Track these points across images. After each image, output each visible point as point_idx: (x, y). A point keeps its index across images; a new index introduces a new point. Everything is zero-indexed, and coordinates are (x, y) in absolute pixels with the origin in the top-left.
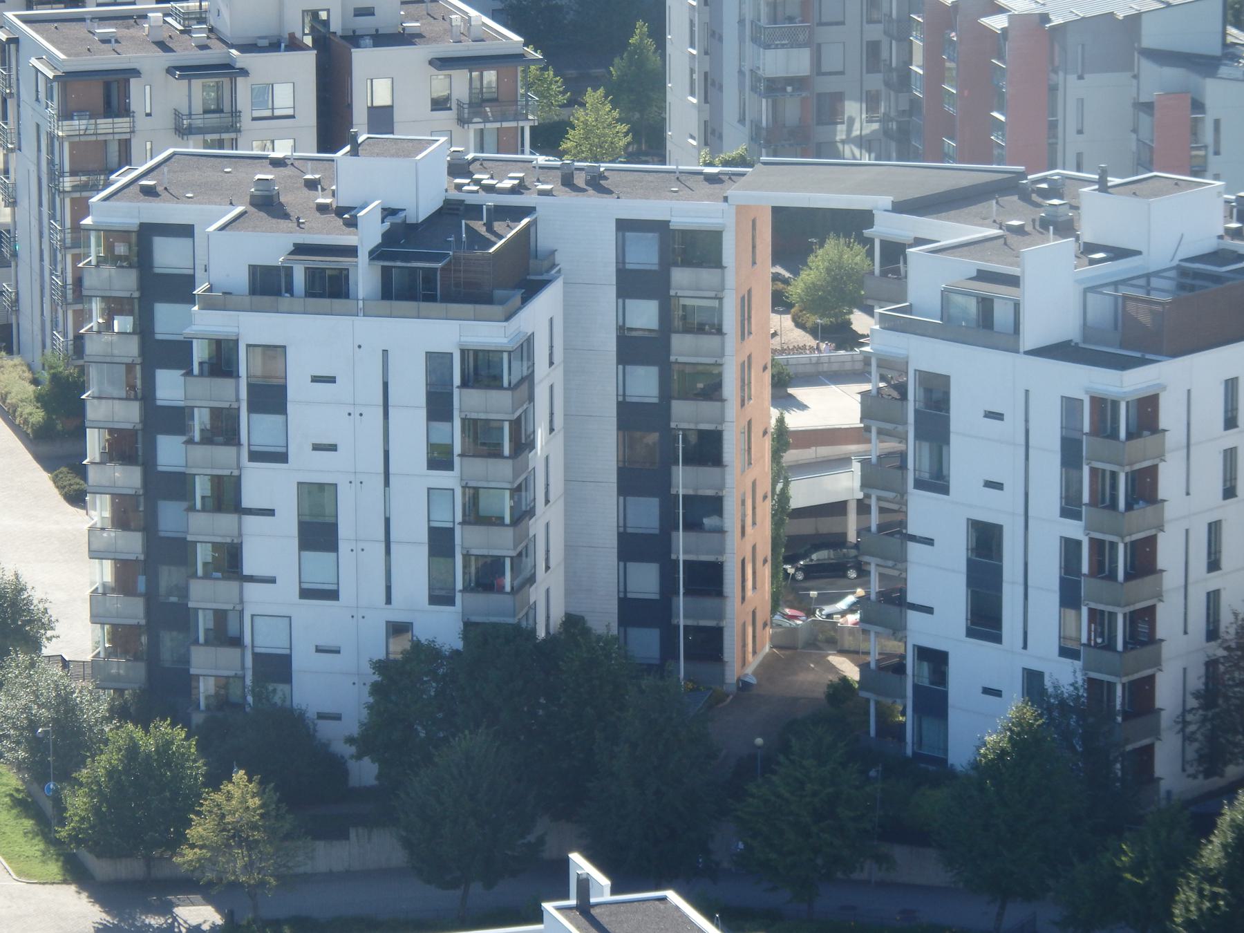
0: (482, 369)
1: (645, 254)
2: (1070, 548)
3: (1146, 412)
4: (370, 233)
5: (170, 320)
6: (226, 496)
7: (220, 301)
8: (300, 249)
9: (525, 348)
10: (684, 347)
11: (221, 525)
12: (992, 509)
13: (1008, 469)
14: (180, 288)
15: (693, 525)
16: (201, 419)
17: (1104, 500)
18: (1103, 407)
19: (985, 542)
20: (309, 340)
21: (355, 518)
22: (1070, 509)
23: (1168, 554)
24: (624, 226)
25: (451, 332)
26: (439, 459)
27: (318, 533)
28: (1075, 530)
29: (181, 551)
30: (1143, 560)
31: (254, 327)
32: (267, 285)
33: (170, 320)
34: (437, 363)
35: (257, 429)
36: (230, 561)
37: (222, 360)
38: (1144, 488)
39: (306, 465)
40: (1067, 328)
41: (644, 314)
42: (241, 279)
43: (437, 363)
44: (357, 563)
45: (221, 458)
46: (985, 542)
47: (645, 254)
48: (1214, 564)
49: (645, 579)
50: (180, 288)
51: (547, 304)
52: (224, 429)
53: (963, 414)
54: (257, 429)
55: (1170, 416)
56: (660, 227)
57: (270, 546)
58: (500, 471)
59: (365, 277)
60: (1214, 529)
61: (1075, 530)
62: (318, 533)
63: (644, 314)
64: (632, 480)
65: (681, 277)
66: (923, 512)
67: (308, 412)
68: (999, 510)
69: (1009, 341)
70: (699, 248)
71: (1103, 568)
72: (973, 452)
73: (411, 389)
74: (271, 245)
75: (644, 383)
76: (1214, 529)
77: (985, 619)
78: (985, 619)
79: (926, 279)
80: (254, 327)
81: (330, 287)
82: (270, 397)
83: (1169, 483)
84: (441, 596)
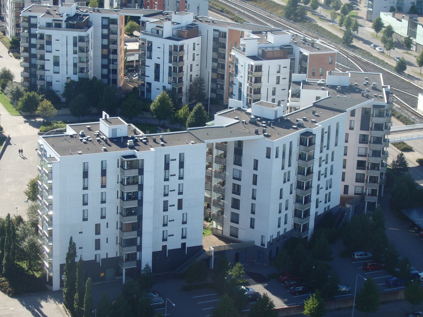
0: (82, 39)
1: (106, 22)
2: (170, 67)
3: (182, 47)
4: (65, 18)
5: (33, 30)
6: (42, 58)
8: (54, 20)
9: (88, 36)
11: (42, 62)
13: (161, 56)
14: (35, 26)
15: (113, 63)
16: (38, 46)
17: (175, 61)
18: (175, 47)
19: (157, 66)
20: (55, 34)
21: (62, 61)
22: (170, 62)
23: (185, 69)
24: (103, 18)
25: (77, 33)
26: (75, 52)
27: (56, 63)
28: (171, 65)
29: (35, 66)
30: (181, 70)
31: (47, 32)
32: (49, 25)
33: (33, 30)
34: (75, 38)
35: (47, 47)
36: (43, 68)
37: (42, 37)
38: (181, 59)
39: (55, 53)
40: (170, 35)
41: (106, 31)
42: (45, 25)
43: (75, 38)
44: (62, 68)
45: (42, 52)
46: (157, 66)
47: (106, 22)
48: (191, 71)
49: (105, 71)
50: (35, 26)
51: (91, 30)
52: (42, 47)
53: (154, 48)
54: (47, 47)
55: (185, 48)
56: (108, 18)
57: (49, 65)
58: (84, 55)
59: (64, 25)
60: (191, 65)
61: (171, 65)
62: (56, 63)
64: (104, 57)
65: (111, 26)
66: (148, 62)
67: (55, 45)
69: (161, 36)
70: (114, 22)
71: (175, 70)
72: (156, 53)
73: (71, 42)
74: (49, 20)
76: (191, 65)
77: (157, 78)
78: (157, 78)
79: (149, 27)
80: (47, 32)
81: (58, 26)
82: (49, 43)
83: (185, 58)
84: (75, 73)
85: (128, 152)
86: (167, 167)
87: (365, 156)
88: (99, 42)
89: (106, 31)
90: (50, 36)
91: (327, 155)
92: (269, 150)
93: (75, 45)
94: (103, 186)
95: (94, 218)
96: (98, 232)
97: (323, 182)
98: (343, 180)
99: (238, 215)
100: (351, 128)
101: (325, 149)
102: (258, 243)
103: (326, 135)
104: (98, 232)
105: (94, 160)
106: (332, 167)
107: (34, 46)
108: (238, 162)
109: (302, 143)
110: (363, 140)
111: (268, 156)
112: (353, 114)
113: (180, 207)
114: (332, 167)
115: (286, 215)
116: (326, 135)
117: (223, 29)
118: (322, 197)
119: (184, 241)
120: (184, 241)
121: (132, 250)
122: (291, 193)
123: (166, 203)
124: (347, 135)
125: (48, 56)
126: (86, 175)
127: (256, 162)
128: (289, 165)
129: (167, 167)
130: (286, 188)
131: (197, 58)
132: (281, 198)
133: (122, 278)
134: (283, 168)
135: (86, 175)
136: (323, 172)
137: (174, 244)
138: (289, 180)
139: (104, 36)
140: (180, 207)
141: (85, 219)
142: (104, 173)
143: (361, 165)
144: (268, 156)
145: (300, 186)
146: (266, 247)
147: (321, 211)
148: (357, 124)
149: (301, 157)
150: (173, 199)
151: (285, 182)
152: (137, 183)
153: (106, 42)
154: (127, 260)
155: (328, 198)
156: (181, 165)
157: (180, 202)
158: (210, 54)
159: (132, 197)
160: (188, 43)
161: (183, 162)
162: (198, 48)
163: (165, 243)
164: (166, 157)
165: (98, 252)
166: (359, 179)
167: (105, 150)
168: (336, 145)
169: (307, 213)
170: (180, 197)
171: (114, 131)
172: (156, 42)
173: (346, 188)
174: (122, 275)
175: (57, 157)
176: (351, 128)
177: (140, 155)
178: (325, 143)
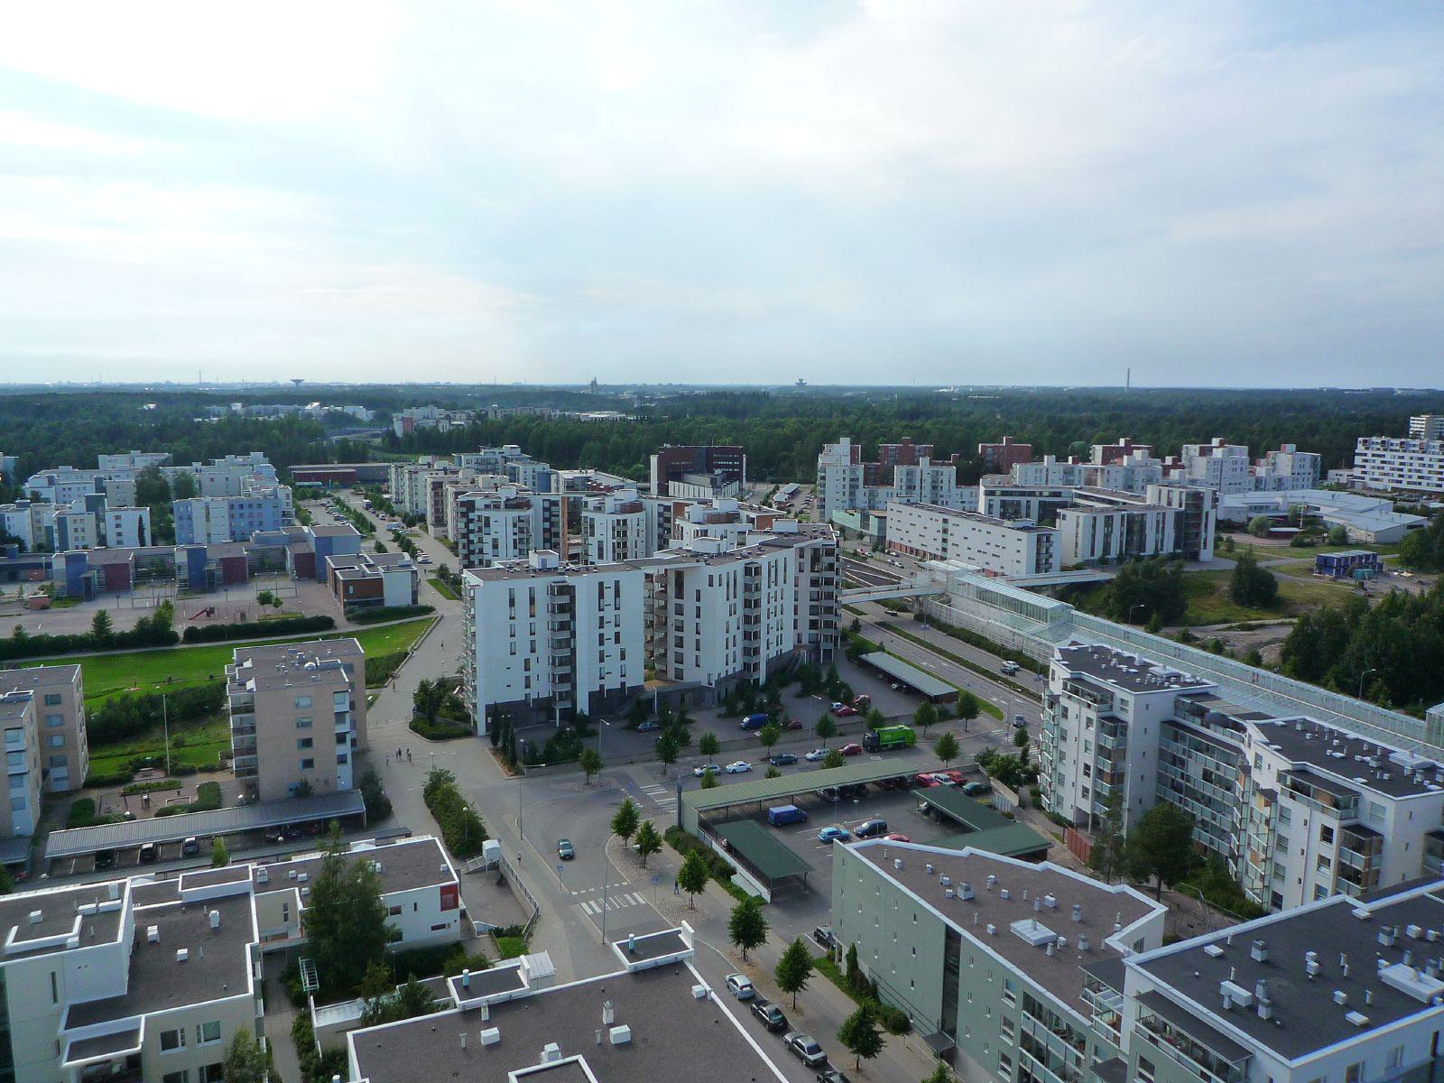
1: (547, 505)
2: (614, 544)
4: (504, 499)
5: (471, 515)
6: (480, 541)
10: (553, 519)
12: (601, 538)
13: (605, 533)
20: (493, 515)
25: (515, 513)
27: (495, 546)
28: (615, 541)
30: (625, 544)
31: (485, 514)
36: (481, 551)
38: (625, 533)
39: (493, 535)
46: (600, 543)
47: (547, 505)
52: (480, 530)
58: (524, 536)
59: (502, 507)
61: (615, 541)
62: (495, 546)
63: (547, 525)
68: (603, 538)
70: (555, 503)
71: (619, 543)
74: (488, 501)
75: (547, 525)
77: (601, 556)
79: (590, 506)
80: (485, 514)
81: (497, 507)
82: (487, 524)
85: (560, 578)
86: (601, 595)
87: (818, 600)
88: (542, 525)
90: (487, 519)
91: (776, 592)
92: (711, 577)
93: (515, 525)
95: (523, 652)
97: (773, 621)
98: (795, 627)
99: (681, 638)
100: (801, 571)
101: (773, 585)
102: (705, 683)
103: (773, 570)
105: (521, 587)
106: (782, 605)
108: (680, 594)
109: (747, 571)
110: (814, 583)
111: (711, 585)
112: (802, 550)
113: (617, 640)
114: (782, 605)
115: (734, 652)
116: (773, 570)
117: (667, 504)
118: (773, 639)
119: (623, 679)
120: (623, 679)
121: (566, 687)
122: (738, 628)
123: (601, 636)
124: (796, 578)
125: (487, 539)
126: (512, 603)
127: (698, 592)
128: (735, 597)
129: (601, 595)
130: (733, 621)
131: (643, 534)
132: (727, 632)
134: (728, 599)
135: (512, 603)
136: (772, 610)
137: (612, 683)
138: (735, 613)
139: (545, 530)
140: (617, 640)
142: (532, 601)
143: (813, 610)
144: (711, 585)
145: (747, 619)
146: (713, 686)
147: (773, 654)
148: (807, 566)
149: (747, 588)
150: (609, 631)
151: (731, 615)
152: (570, 629)
153: (548, 535)
154: (561, 699)
155: (779, 641)
156: (617, 594)
157: (617, 635)
158: (656, 531)
160: (632, 518)
161: (619, 591)
162: (643, 524)
163: (602, 682)
164: (601, 584)
165: (528, 691)
166: (813, 625)
167: (533, 577)
168: (785, 582)
169: (756, 651)
170: (617, 629)
171: (544, 561)
172: (598, 518)
173: (799, 636)
176: (801, 571)
178: (773, 579)
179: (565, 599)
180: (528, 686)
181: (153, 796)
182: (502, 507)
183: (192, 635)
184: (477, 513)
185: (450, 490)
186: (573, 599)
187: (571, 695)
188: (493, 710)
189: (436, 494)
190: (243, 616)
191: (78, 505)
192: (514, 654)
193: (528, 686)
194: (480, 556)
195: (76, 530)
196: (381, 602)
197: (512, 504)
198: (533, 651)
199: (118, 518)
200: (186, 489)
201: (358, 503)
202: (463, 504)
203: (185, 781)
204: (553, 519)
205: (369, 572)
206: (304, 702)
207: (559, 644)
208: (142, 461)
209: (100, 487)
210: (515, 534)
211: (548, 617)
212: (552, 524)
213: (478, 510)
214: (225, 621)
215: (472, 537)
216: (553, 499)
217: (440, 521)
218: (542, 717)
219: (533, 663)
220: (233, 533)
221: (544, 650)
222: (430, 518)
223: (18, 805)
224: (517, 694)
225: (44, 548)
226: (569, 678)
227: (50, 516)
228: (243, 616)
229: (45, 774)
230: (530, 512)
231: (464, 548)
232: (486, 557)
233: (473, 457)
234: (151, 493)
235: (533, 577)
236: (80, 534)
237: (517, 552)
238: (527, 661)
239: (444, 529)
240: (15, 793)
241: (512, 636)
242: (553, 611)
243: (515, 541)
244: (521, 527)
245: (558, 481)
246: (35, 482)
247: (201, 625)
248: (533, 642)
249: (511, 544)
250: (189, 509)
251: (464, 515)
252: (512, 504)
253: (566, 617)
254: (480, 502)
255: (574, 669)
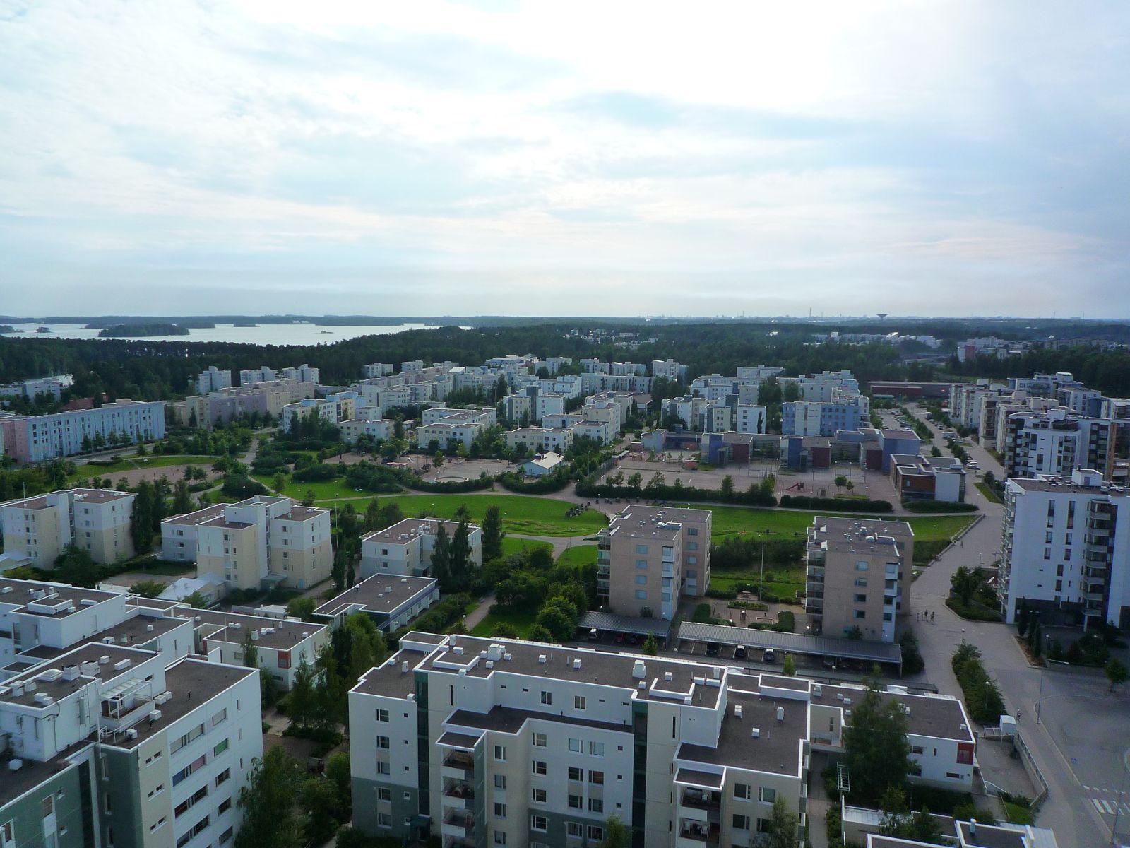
4: (1052, 420)
6: (1026, 455)
7: (1029, 428)
8: (1041, 422)
11: (1025, 459)
16: (1024, 445)
20: (1040, 433)
21: (1045, 459)
24: (1092, 424)
25: (1063, 434)
26: (1060, 452)
27: (1040, 460)
32: (1035, 426)
36: (1026, 464)
39: (1039, 451)
41: (1094, 438)
42: (1031, 426)
44: (1045, 464)
47: (1095, 428)
52: (1027, 445)
56: (1098, 424)
58: (1070, 454)
59: (1050, 426)
62: (1040, 460)
63: (1094, 447)
65: (1101, 432)
70: (1104, 428)
74: (1037, 421)
75: (1094, 447)
81: (1045, 426)
85: (1103, 497)
89: (1094, 438)
90: (1035, 437)
93: (1061, 444)
94: (1070, 527)
95: (1057, 558)
96: (1060, 573)
104: (1060, 573)
105: (1062, 501)
107: (1019, 446)
121: (1098, 597)
125: (1031, 453)
126: (1051, 513)
133: (1083, 627)
135: (1051, 513)
139: (1091, 451)
141: (1047, 558)
142: (1071, 514)
154: (1091, 607)
159: (1101, 541)
165: (1058, 594)
167: (1075, 492)
171: (1087, 480)
174: (1083, 624)
175: (1023, 491)
177: (1112, 500)
179: (1106, 517)
180: (1059, 588)
181: (749, 613)
182: (1050, 426)
183: (787, 502)
184: (1025, 430)
185: (1002, 408)
186: (1114, 518)
187: (1103, 606)
188: (1022, 604)
189: (990, 412)
190: (823, 492)
191: (721, 401)
192: (1048, 558)
193: (1059, 588)
194: (1024, 468)
195: (718, 418)
196: (933, 496)
197: (1058, 425)
198: (1067, 558)
199: (746, 412)
200: (793, 395)
201: (921, 414)
202: (1013, 421)
203: (771, 606)
204: (1101, 442)
205: (924, 471)
206: (863, 566)
207: (1095, 557)
208: (765, 372)
209: (736, 390)
210: (1060, 452)
211: (1086, 530)
212: (1099, 447)
213: (1026, 427)
214: (809, 494)
215: (1018, 450)
216: (1102, 423)
217: (991, 434)
218: (1070, 619)
219: (1066, 570)
220: (822, 430)
221: (1078, 559)
222: (982, 431)
223: (665, 598)
224: (1048, 594)
225: (698, 429)
226: (1104, 590)
227: (703, 407)
228: (823, 492)
229: (683, 581)
230: (1077, 434)
231: (1010, 459)
232: (1030, 470)
233: (1027, 382)
234: (769, 396)
235: (1075, 492)
236: (720, 421)
237: (1060, 468)
238: (1060, 568)
239: (994, 441)
240: (665, 590)
241: (1048, 542)
242: (1092, 526)
243: (1059, 457)
244: (1067, 447)
245: (1109, 408)
246: (697, 384)
247: (793, 495)
248: (1068, 551)
249: (1055, 460)
250: (794, 409)
251: (1013, 431)
252: (1058, 425)
253: (1105, 533)
254: (1029, 421)
255: (1108, 582)
